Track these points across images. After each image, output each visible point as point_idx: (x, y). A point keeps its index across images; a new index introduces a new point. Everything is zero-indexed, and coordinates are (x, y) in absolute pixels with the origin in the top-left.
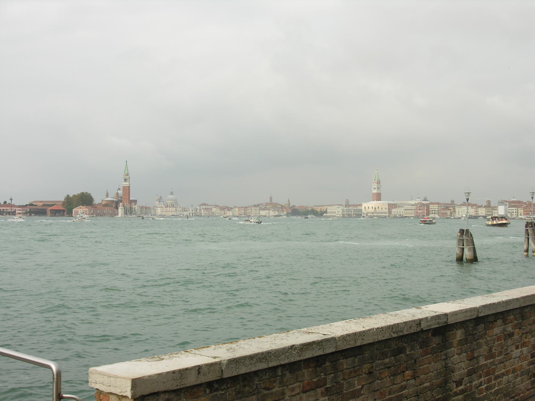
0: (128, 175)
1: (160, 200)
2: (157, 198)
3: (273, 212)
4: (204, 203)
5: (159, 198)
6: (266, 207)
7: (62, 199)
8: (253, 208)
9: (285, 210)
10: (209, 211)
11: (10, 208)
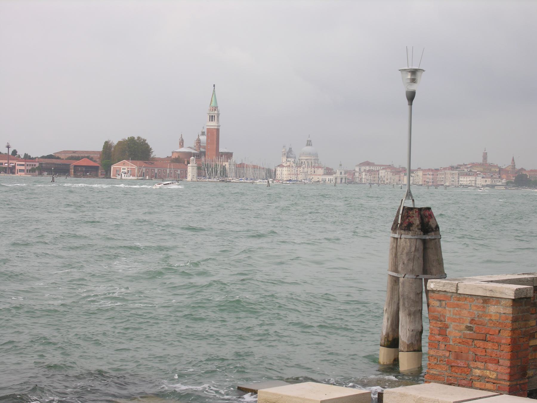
0: (216, 108)
1: (289, 154)
2: (284, 150)
3: (483, 179)
5: (288, 150)
6: (470, 171)
7: (100, 148)
9: (504, 176)
10: (374, 174)
11: (6, 161)
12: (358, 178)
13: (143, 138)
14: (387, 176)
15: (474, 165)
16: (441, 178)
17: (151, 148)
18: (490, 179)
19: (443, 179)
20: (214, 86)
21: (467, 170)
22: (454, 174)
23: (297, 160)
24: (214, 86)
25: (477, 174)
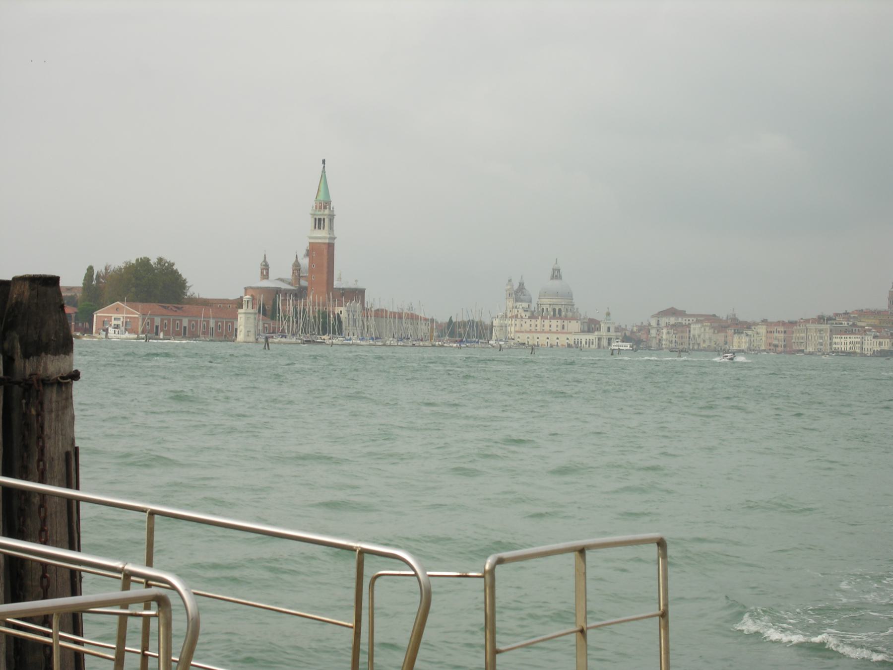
0: (326, 204)
2: (509, 287)
3: (875, 340)
4: (673, 308)
5: (516, 287)
6: (854, 325)
8: (811, 326)
10: (682, 332)
13: (168, 261)
14: (704, 335)
15: (862, 313)
16: (798, 338)
17: (185, 280)
18: (888, 340)
19: (802, 341)
20: (324, 162)
21: (848, 324)
22: (822, 330)
23: (534, 305)
24: (324, 162)
25: (865, 331)
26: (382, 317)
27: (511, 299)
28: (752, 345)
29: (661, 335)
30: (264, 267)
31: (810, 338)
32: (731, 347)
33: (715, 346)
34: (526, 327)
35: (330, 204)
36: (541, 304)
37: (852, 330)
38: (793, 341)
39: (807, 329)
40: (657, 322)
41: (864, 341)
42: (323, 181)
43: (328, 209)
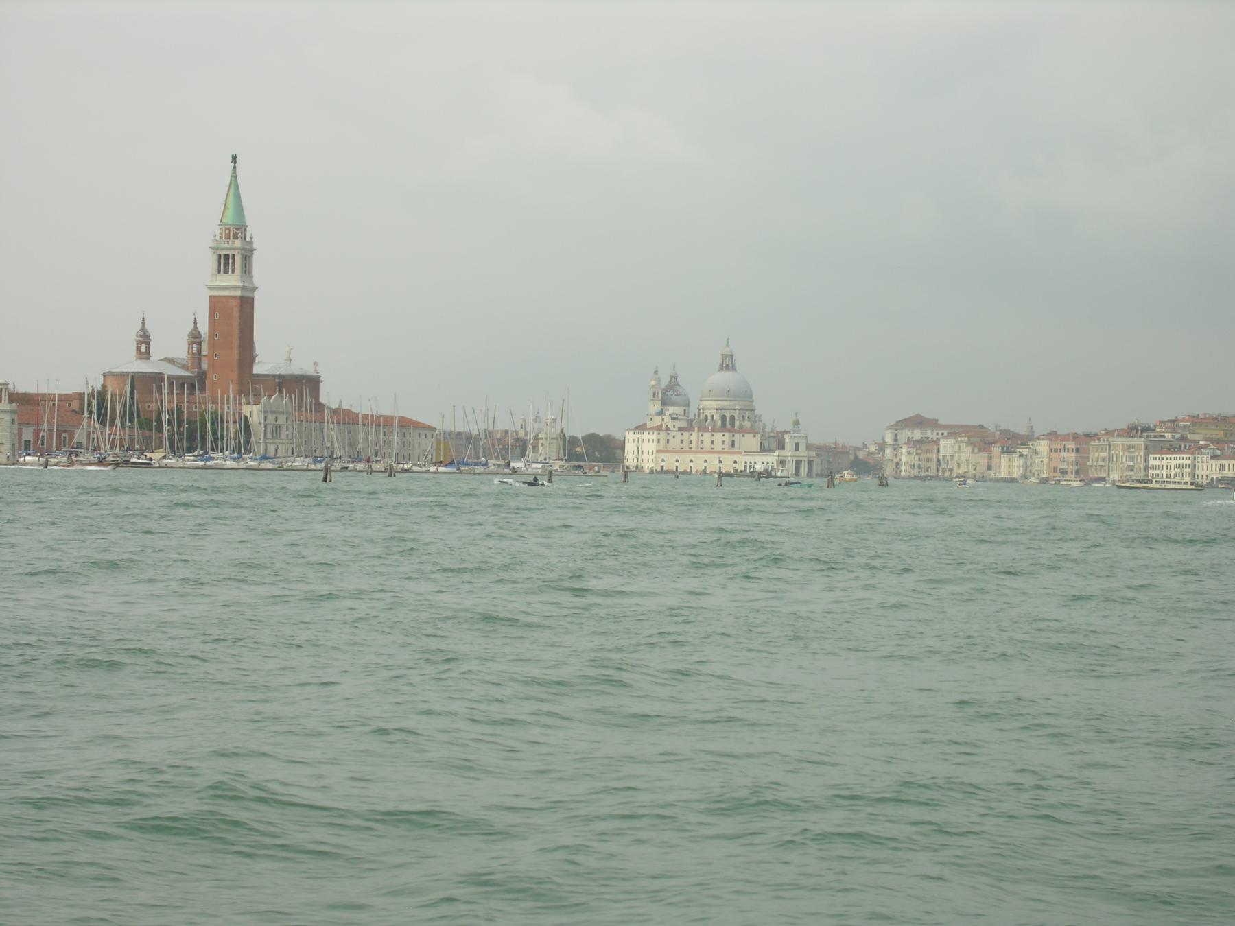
6: (1183, 438)
10: (928, 451)
12: (890, 463)
14: (959, 456)
15: (1197, 421)
16: (1097, 459)
19: (1102, 464)
21: (1173, 436)
22: (1133, 447)
23: (693, 411)
25: (1199, 448)
26: (348, 424)
27: (657, 402)
28: (1028, 470)
29: (899, 457)
30: (141, 339)
31: (1115, 459)
32: (998, 474)
33: (974, 472)
34: (675, 443)
35: (245, 230)
36: (703, 409)
37: (1180, 446)
38: (1089, 464)
39: (1110, 446)
40: (893, 437)
41: (1197, 464)
42: (232, 191)
43: (239, 239)
